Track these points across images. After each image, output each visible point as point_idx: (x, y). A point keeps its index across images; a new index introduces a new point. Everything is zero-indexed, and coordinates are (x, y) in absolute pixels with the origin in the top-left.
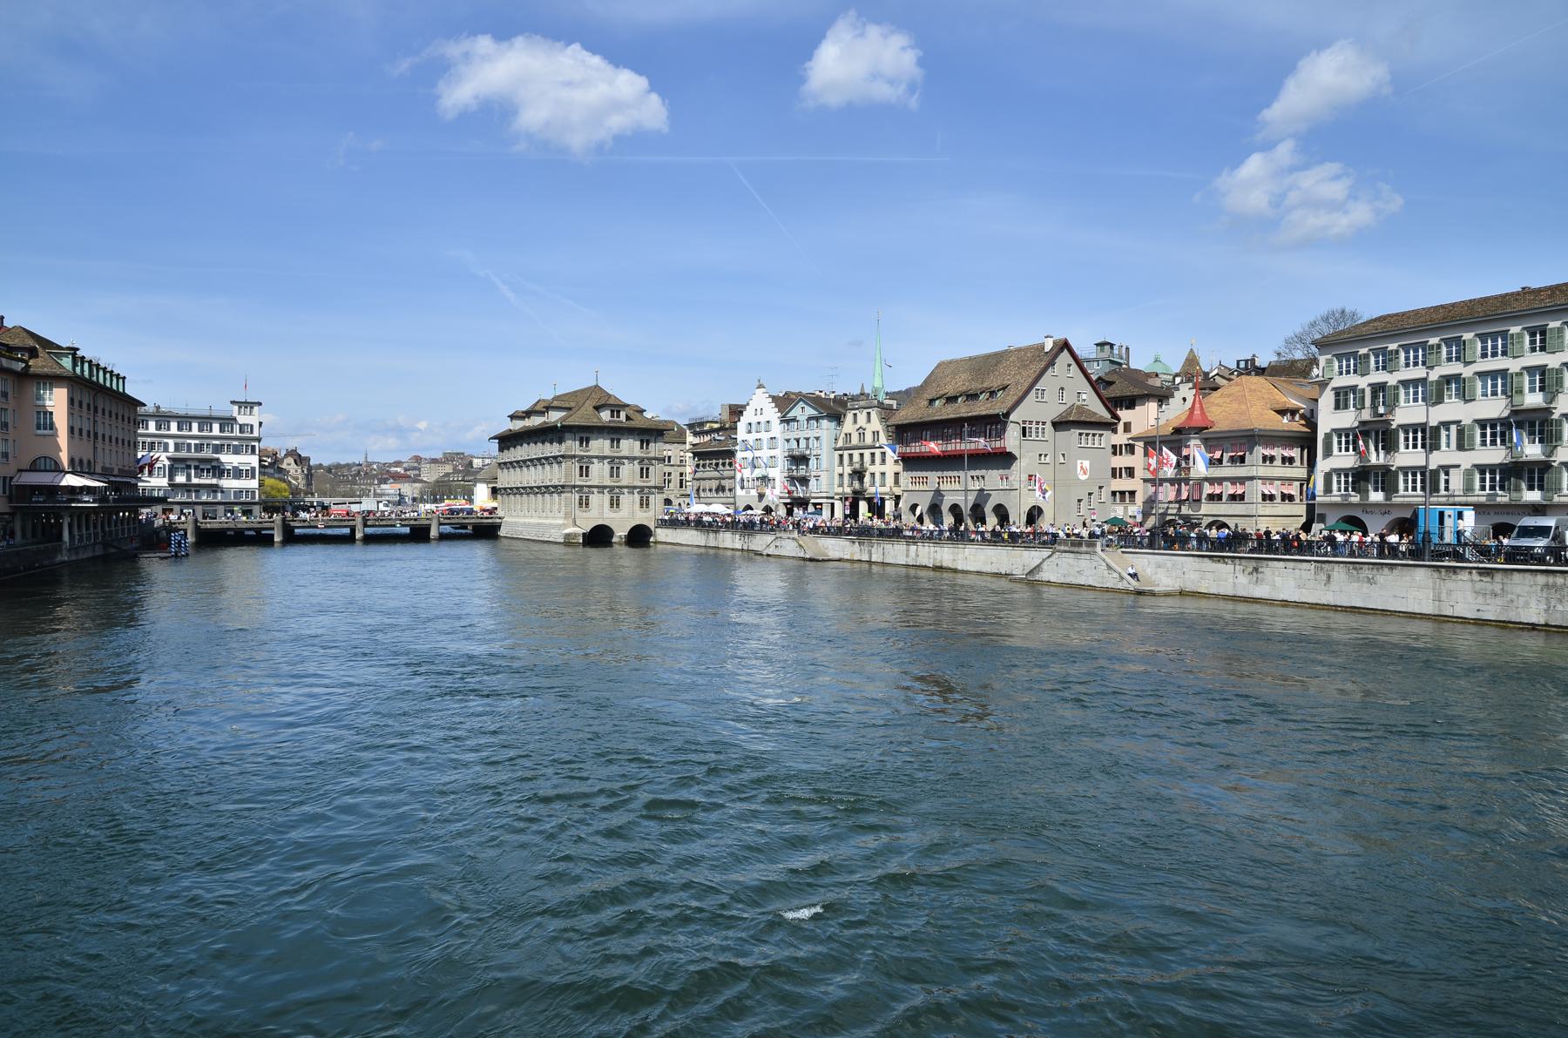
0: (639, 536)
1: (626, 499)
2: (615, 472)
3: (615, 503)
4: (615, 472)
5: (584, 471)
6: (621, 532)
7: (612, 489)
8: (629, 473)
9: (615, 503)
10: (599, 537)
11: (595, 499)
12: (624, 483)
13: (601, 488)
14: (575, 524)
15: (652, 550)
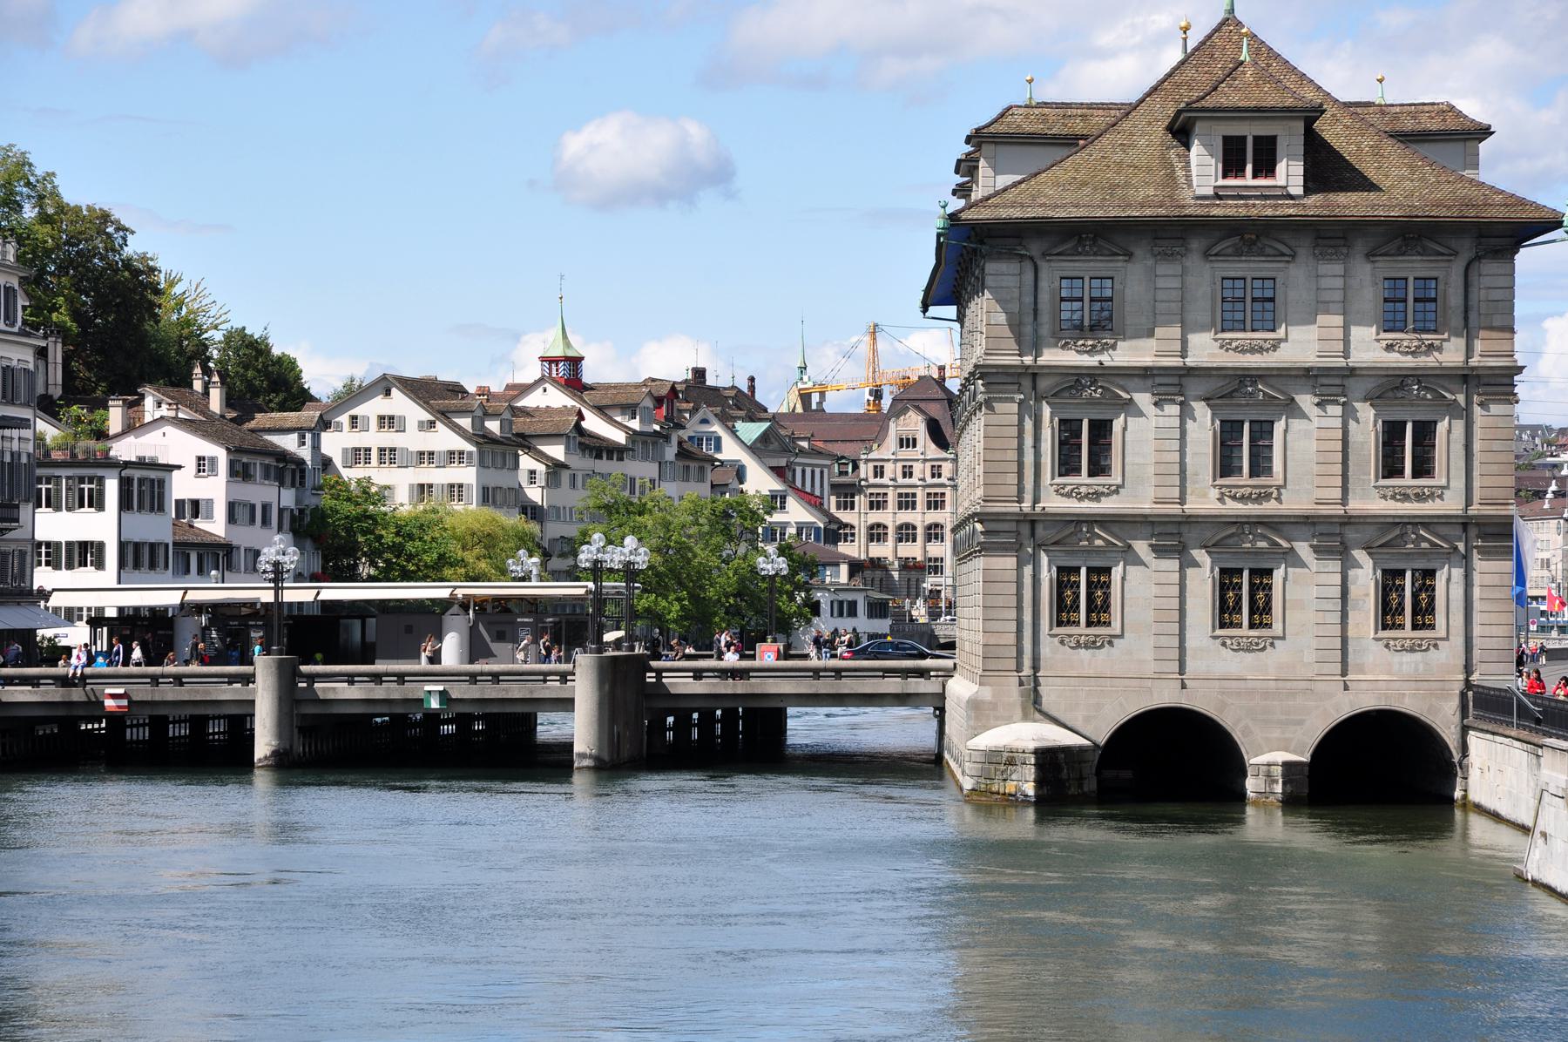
0: (1383, 773)
1: (1304, 587)
2: (1243, 445)
3: (1244, 600)
4: (1243, 445)
5: (1087, 446)
6: (1271, 752)
7: (1221, 533)
8: (1314, 456)
9: (1244, 600)
10: (1167, 767)
11: (1141, 584)
12: (1295, 502)
13: (1173, 534)
14: (1034, 705)
15: (1449, 848)
